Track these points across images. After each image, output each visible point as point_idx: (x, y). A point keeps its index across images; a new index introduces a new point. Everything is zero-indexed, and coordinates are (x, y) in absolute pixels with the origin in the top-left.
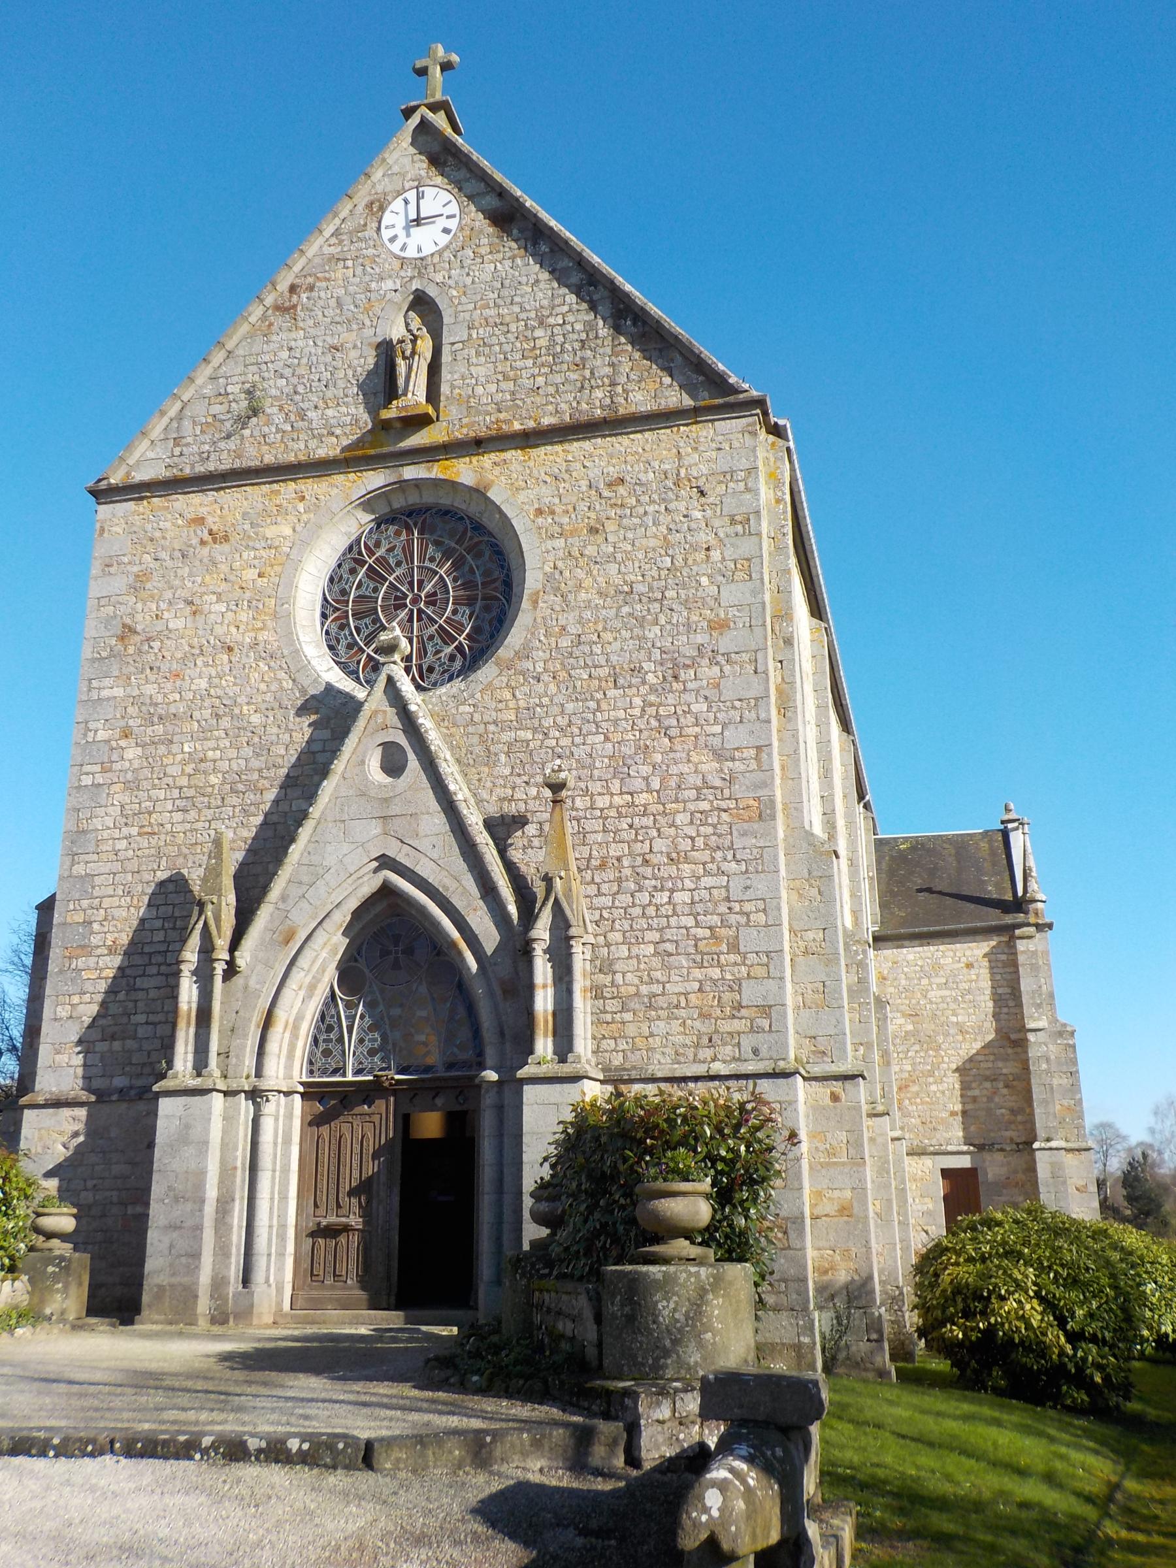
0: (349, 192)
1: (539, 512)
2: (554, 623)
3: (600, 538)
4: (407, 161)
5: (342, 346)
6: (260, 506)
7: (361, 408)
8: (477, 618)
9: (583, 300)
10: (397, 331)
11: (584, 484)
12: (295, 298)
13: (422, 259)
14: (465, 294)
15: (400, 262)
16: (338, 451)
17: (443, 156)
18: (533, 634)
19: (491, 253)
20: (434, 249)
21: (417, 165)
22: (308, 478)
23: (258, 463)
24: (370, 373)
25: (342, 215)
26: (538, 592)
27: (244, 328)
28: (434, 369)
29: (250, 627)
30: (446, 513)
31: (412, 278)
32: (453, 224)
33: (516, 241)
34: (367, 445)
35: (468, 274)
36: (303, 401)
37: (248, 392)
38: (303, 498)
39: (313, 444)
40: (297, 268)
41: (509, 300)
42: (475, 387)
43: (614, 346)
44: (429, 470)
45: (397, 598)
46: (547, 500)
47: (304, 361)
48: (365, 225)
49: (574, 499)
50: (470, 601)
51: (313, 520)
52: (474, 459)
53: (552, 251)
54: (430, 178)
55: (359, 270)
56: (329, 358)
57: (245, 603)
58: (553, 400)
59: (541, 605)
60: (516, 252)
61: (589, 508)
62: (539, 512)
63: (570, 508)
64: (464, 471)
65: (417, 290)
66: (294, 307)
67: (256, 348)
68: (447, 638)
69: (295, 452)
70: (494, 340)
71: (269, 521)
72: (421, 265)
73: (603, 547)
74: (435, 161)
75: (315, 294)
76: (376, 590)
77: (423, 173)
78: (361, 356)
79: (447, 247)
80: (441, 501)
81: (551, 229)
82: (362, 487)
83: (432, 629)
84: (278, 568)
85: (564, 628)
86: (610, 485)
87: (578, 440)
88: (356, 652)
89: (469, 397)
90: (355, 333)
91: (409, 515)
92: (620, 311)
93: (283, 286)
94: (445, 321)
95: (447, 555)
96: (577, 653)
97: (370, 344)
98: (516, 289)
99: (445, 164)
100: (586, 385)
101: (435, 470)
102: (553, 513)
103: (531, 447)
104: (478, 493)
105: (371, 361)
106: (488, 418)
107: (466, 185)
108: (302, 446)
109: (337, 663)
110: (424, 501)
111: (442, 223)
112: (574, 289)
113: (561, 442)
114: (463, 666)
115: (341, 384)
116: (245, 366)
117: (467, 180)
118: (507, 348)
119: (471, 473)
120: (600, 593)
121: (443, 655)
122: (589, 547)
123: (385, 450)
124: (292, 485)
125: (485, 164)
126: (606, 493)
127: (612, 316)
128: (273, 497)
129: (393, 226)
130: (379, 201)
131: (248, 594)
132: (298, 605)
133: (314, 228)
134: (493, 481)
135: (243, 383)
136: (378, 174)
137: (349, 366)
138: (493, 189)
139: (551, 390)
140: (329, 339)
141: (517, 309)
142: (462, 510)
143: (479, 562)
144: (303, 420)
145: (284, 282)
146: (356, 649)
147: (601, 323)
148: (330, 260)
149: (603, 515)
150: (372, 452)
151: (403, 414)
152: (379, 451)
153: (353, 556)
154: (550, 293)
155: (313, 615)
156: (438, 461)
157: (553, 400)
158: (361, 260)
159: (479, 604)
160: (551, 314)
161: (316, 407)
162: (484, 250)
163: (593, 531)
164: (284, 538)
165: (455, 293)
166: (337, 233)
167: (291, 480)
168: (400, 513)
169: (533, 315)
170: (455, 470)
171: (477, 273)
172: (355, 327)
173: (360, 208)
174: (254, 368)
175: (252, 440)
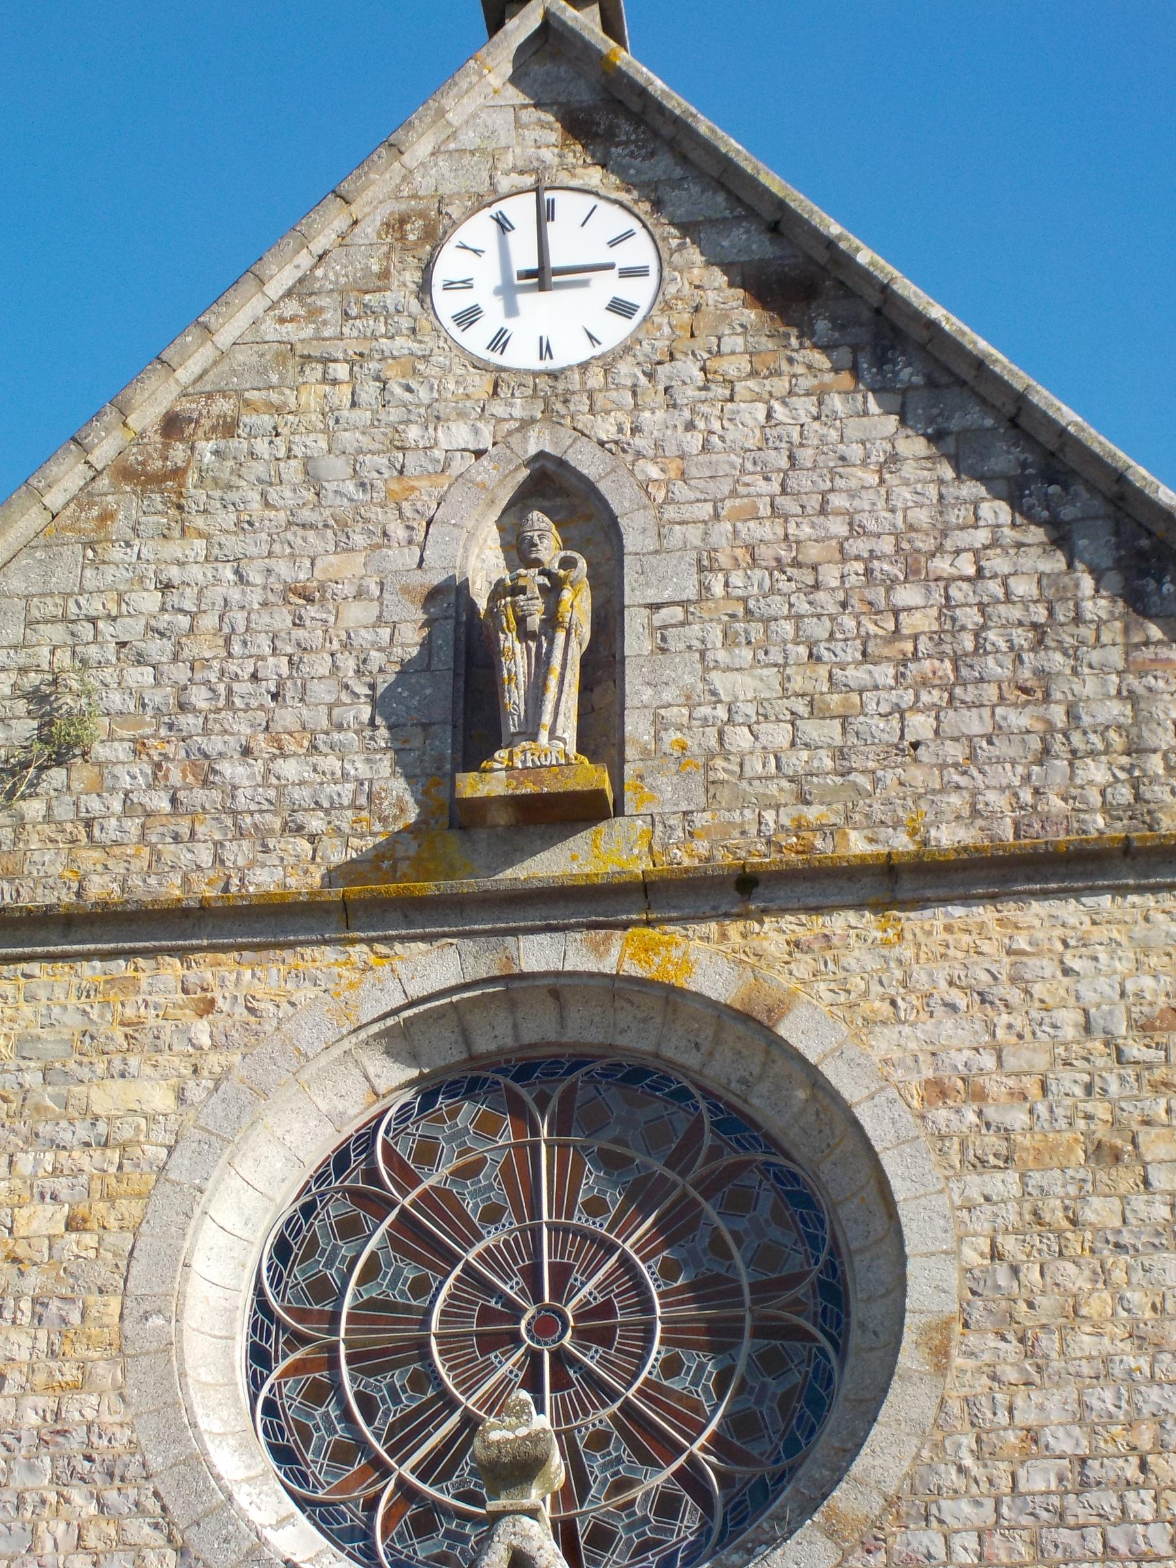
0: (345, 188)
1: (938, 1090)
2: (1003, 1418)
3: (1126, 1179)
4: (502, 121)
5: (322, 588)
6: (74, 1020)
7: (385, 764)
8: (742, 1387)
9: (1032, 519)
10: (483, 566)
11: (1069, 1018)
12: (179, 452)
13: (553, 375)
14: (683, 475)
15: (489, 378)
16: (317, 880)
17: (605, 117)
18: (938, 1446)
19: (754, 373)
20: (586, 352)
21: (531, 135)
22: (225, 949)
23: (68, 898)
24: (406, 669)
25: (317, 247)
26: (947, 1324)
27: (30, 521)
28: (602, 668)
29: (40, 1378)
30: (637, 1075)
31: (526, 424)
32: (640, 292)
33: (826, 348)
34: (404, 867)
35: (690, 426)
36: (206, 732)
37: (37, 697)
38: (207, 1007)
39: (238, 853)
40: (185, 374)
41: (814, 502)
42: (721, 728)
43: (1130, 648)
44: (598, 949)
45: (487, 1315)
46: (959, 1059)
47: (209, 621)
48: (385, 274)
49: (1041, 1061)
50: (720, 1338)
51: (240, 1071)
52: (734, 929)
53: (931, 383)
54: (571, 170)
55: (369, 392)
56: (282, 619)
57: (26, 1305)
58: (963, 781)
59: (958, 1361)
60: (829, 377)
61: (1089, 1089)
62: (938, 1090)
63: (1032, 1086)
64: (706, 961)
65: (541, 455)
66: (178, 473)
67: (61, 579)
68: (652, 1445)
69: (186, 871)
70: (777, 606)
71: (100, 1068)
72: (552, 388)
73: (1139, 1202)
74: (580, 127)
75: (238, 445)
76: (420, 1287)
77: (549, 155)
78: (380, 620)
79: (627, 349)
80: (623, 1041)
81: (933, 325)
82: (393, 984)
83: (603, 1416)
84: (131, 1208)
85: (1032, 1435)
86: (1144, 1028)
87: (1045, 895)
88: (363, 1474)
89: (711, 755)
90: (360, 559)
91: (524, 1073)
92: (1141, 554)
93: (147, 414)
94: (631, 542)
95: (642, 1195)
96: (1077, 1510)
97: (406, 590)
98: (833, 473)
99: (609, 138)
100: (1058, 745)
101: (615, 952)
102: (979, 1095)
103: (904, 905)
104: (752, 1026)
105: (411, 638)
106: (769, 816)
107: (670, 195)
108: (205, 856)
109: (302, 1503)
110: (570, 1036)
111: (607, 286)
112: (1002, 486)
113: (993, 898)
114: (704, 1532)
115: (322, 692)
116: (28, 624)
117: (677, 184)
118: (820, 630)
119: (724, 966)
120: (1137, 1338)
121: (638, 1493)
122: (1096, 1201)
123: (468, 885)
124: (172, 968)
125: (731, 145)
126: (1135, 1050)
127: (1119, 565)
128: (114, 996)
129: (467, 284)
130: (422, 215)
131: (33, 1281)
132: (192, 1319)
133: (249, 271)
134: (793, 994)
135: (23, 671)
136: (420, 148)
137: (346, 646)
138: (752, 213)
139: (955, 752)
140: (283, 569)
141: (838, 527)
142: (684, 1069)
143: (743, 1224)
144: (206, 784)
145: (151, 404)
146: (360, 1463)
147: (1087, 583)
148: (281, 359)
149: (1132, 1114)
150: (429, 888)
151: (528, 789)
152: (448, 886)
153: (352, 1177)
154: (932, 491)
155: (227, 1353)
156: (625, 926)
157: (963, 781)
158: (374, 365)
159: (747, 1344)
160: (940, 548)
161: (246, 752)
162: (734, 366)
163: (1104, 1154)
164: (150, 1118)
165: (654, 472)
166: (300, 289)
167: (170, 952)
168: (483, 1067)
169: (886, 545)
170: (676, 954)
171: (716, 426)
172: (359, 540)
173: (369, 229)
174: (57, 633)
175: (48, 830)
